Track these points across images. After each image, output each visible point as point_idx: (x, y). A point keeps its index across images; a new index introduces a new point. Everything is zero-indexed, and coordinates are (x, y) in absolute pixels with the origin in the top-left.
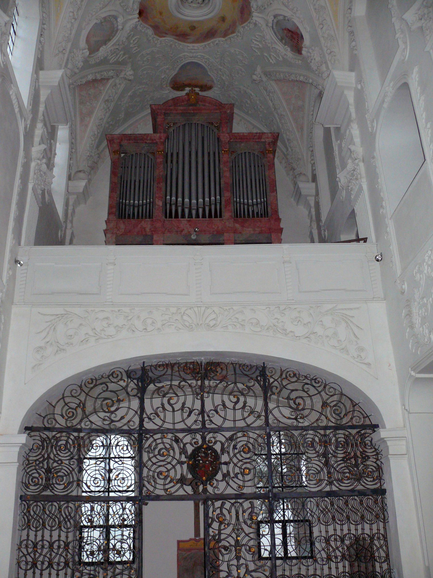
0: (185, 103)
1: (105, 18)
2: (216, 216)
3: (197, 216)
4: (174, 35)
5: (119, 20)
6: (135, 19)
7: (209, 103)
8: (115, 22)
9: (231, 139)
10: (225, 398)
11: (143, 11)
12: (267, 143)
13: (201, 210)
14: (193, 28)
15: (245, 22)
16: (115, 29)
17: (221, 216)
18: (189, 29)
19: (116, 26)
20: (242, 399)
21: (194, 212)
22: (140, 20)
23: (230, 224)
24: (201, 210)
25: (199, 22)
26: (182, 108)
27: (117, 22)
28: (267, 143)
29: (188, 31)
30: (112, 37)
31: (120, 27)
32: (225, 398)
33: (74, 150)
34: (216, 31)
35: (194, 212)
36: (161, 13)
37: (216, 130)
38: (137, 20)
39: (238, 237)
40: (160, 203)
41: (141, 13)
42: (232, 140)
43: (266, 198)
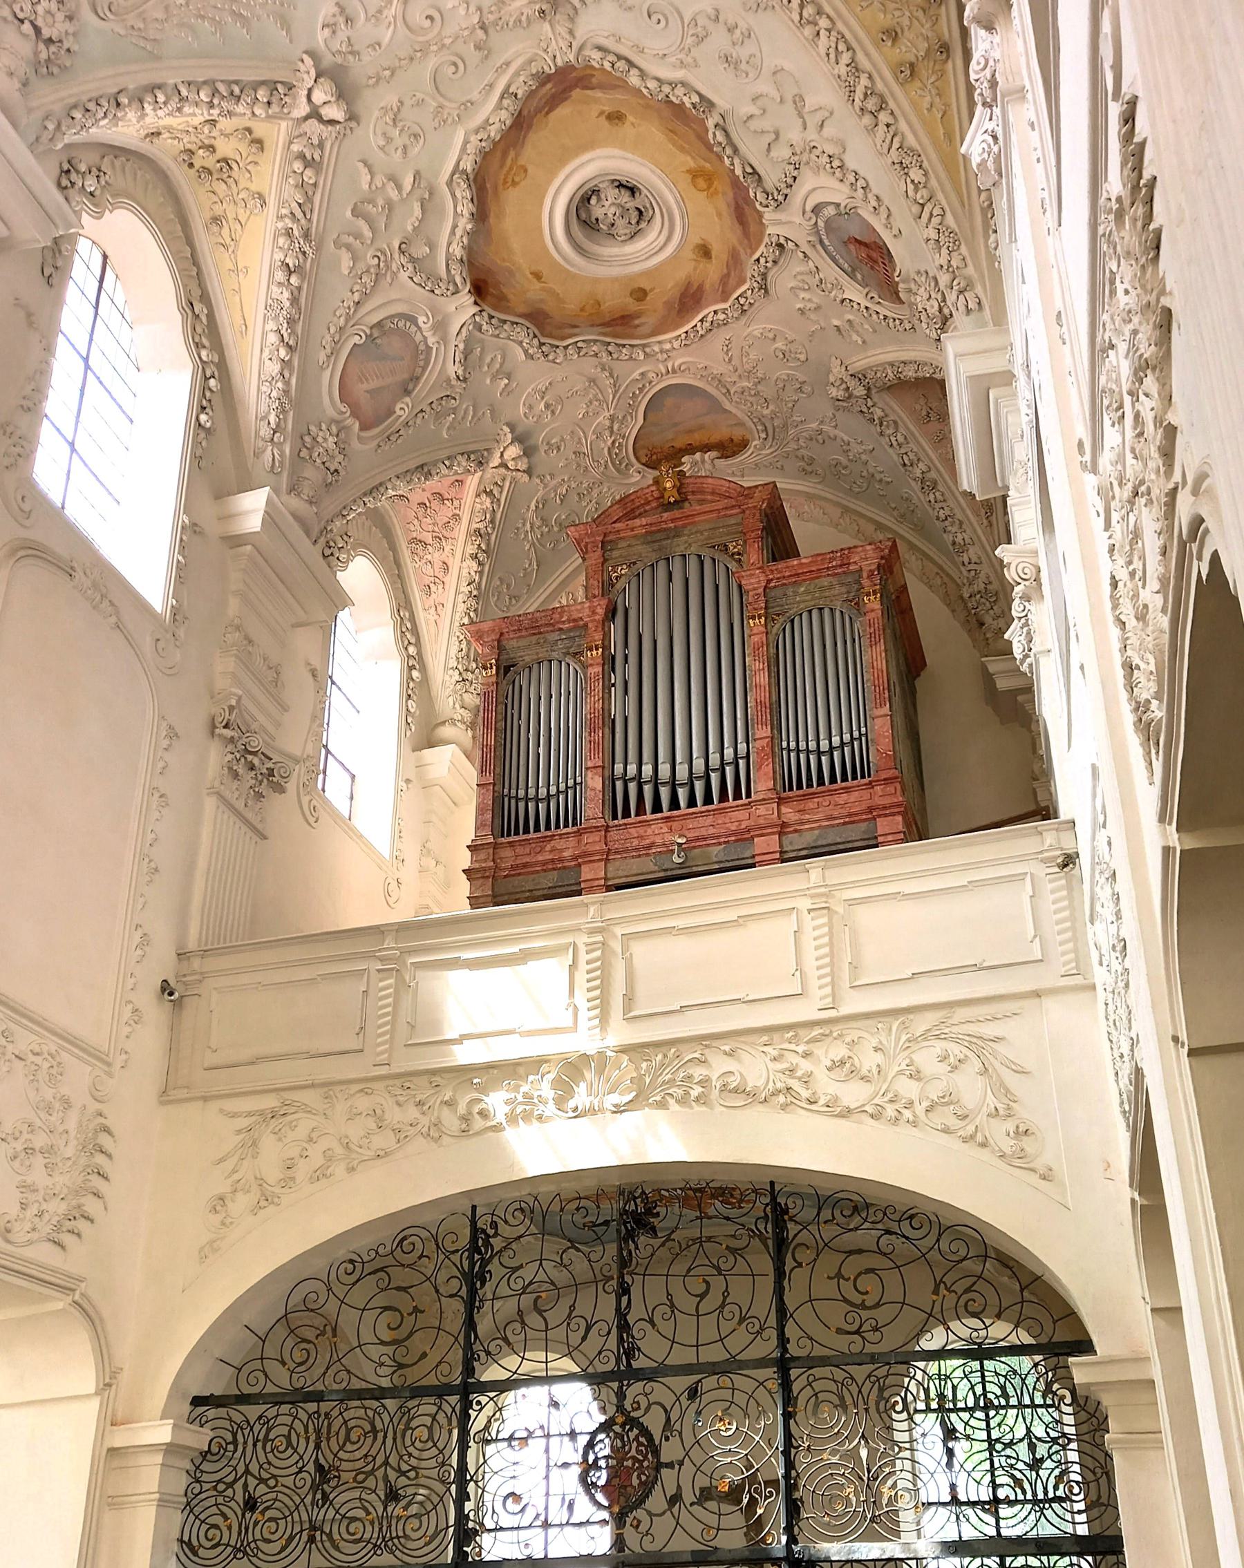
0: (654, 504)
1: (379, 324)
2: (738, 796)
3: (692, 802)
4: (592, 326)
5: (421, 319)
6: (462, 309)
7: (713, 493)
8: (413, 329)
9: (769, 581)
10: (676, 1286)
11: (485, 282)
12: (865, 575)
13: (699, 786)
14: (641, 294)
15: (757, 249)
16: (422, 347)
17: (749, 795)
18: (631, 300)
19: (418, 338)
20: (718, 1283)
21: (682, 794)
22: (485, 307)
23: (766, 812)
24: (699, 786)
25: (647, 273)
26: (644, 521)
27: (420, 328)
28: (865, 575)
29: (633, 306)
30: (419, 370)
31: (431, 340)
32: (676, 1286)
33: (415, 674)
34: (700, 288)
35: (682, 794)
36: (538, 276)
37: (733, 566)
38: (476, 309)
39: (791, 843)
40: (595, 782)
41: (480, 290)
42: (772, 584)
43: (866, 726)
